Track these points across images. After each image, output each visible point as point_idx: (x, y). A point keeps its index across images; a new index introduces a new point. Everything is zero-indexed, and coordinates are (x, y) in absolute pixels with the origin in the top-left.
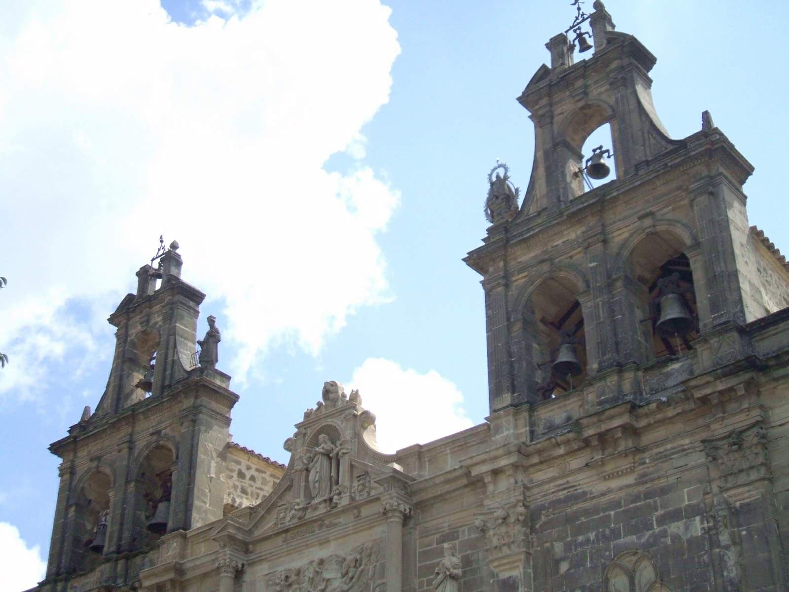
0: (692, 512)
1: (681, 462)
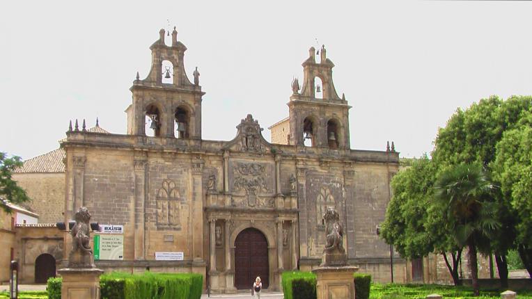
0: (337, 182)
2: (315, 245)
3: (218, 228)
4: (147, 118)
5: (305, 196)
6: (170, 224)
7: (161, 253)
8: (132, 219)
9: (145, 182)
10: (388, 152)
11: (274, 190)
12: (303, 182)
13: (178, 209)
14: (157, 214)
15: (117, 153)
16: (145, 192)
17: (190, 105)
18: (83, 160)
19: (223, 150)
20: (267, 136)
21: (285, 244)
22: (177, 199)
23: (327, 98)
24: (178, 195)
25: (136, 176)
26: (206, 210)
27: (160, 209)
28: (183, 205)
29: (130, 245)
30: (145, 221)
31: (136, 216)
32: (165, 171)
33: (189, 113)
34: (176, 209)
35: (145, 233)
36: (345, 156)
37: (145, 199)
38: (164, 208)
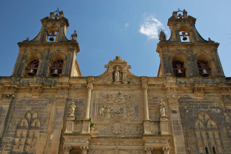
0: (217, 108)
1: (214, 98)
14: (13, 143)
22: (36, 128)
23: (193, 41)
24: (39, 124)
27: (17, 137)
28: (42, 134)
34: (34, 137)
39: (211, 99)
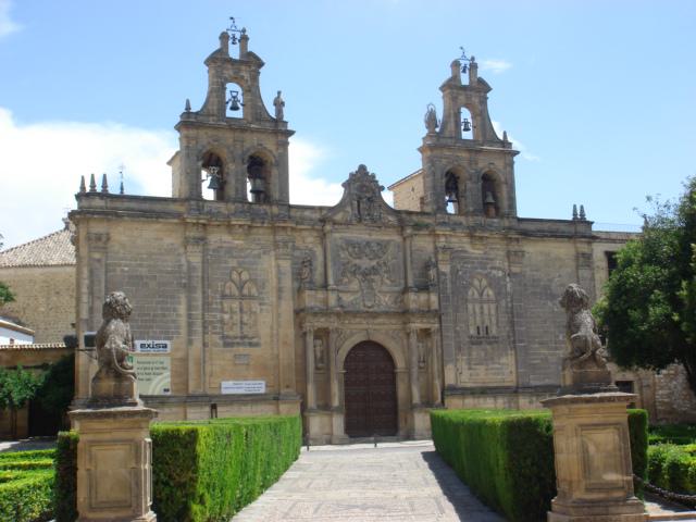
0: (499, 269)
2: (467, 367)
3: (319, 342)
4: (204, 174)
5: (449, 291)
6: (243, 337)
7: (231, 383)
8: (184, 331)
9: (203, 272)
10: (575, 222)
11: (403, 281)
12: (445, 268)
13: (255, 313)
14: (222, 321)
15: (158, 226)
16: (203, 287)
17: (271, 151)
18: (104, 239)
19: (323, 221)
20: (388, 197)
21: (422, 365)
22: (251, 297)
24: (254, 291)
25: (189, 262)
26: (297, 312)
28: (264, 307)
29: (181, 371)
30: (204, 333)
31: (190, 325)
32: (235, 254)
33: (268, 165)
34: (251, 312)
35: (204, 351)
36: (510, 228)
37: (204, 298)
38: (232, 312)
39: (492, 254)
